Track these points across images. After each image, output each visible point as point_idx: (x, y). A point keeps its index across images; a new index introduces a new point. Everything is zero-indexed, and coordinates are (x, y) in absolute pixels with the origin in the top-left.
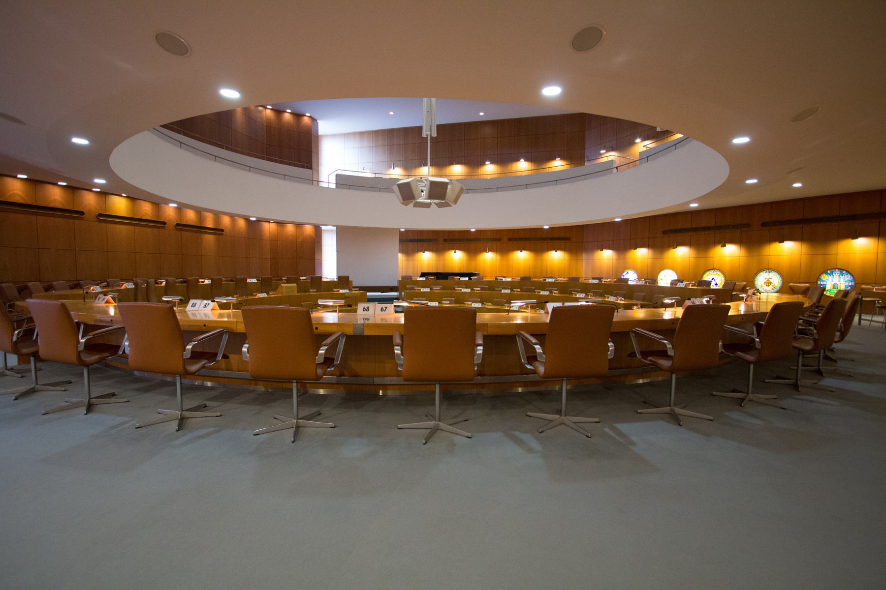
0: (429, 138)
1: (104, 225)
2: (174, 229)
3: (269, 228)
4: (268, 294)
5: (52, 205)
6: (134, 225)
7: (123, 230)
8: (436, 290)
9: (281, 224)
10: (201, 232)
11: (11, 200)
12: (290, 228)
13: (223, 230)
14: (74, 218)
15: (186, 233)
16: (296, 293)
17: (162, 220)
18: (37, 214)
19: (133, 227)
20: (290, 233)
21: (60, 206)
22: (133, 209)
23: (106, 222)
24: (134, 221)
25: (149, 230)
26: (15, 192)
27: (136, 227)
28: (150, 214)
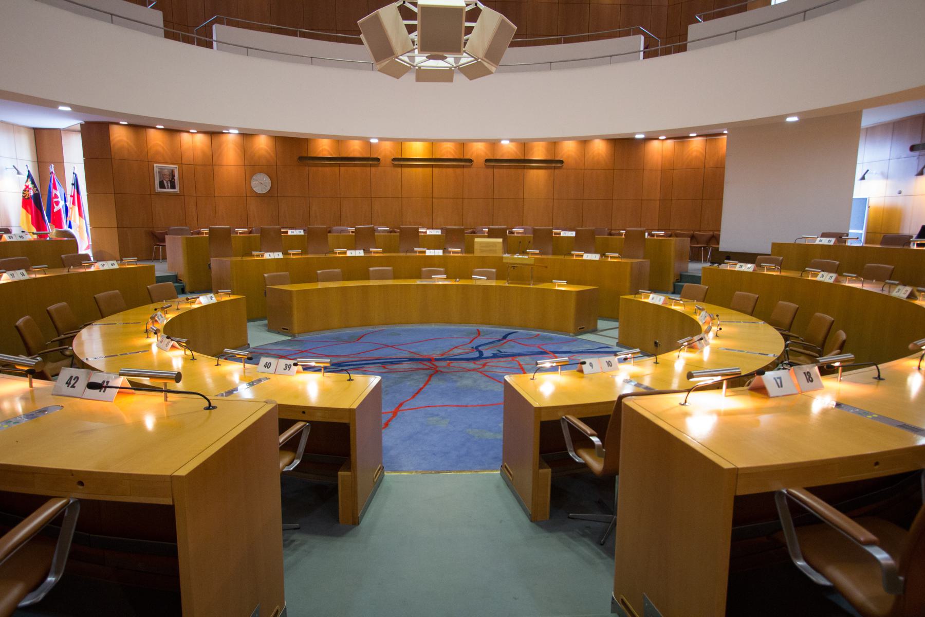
1: (399, 170)
2: (484, 166)
3: (660, 149)
4: (445, 250)
5: (351, 155)
6: (432, 166)
7: (418, 173)
8: (454, 252)
9: (681, 137)
10: (524, 168)
11: (321, 155)
12: (696, 144)
13: (562, 162)
14: (371, 165)
15: (501, 171)
16: (499, 252)
18: (339, 165)
19: (431, 169)
20: (694, 154)
21: (358, 155)
23: (402, 166)
24: (433, 162)
25: (450, 170)
26: (324, 147)
27: (434, 169)
28: (452, 151)
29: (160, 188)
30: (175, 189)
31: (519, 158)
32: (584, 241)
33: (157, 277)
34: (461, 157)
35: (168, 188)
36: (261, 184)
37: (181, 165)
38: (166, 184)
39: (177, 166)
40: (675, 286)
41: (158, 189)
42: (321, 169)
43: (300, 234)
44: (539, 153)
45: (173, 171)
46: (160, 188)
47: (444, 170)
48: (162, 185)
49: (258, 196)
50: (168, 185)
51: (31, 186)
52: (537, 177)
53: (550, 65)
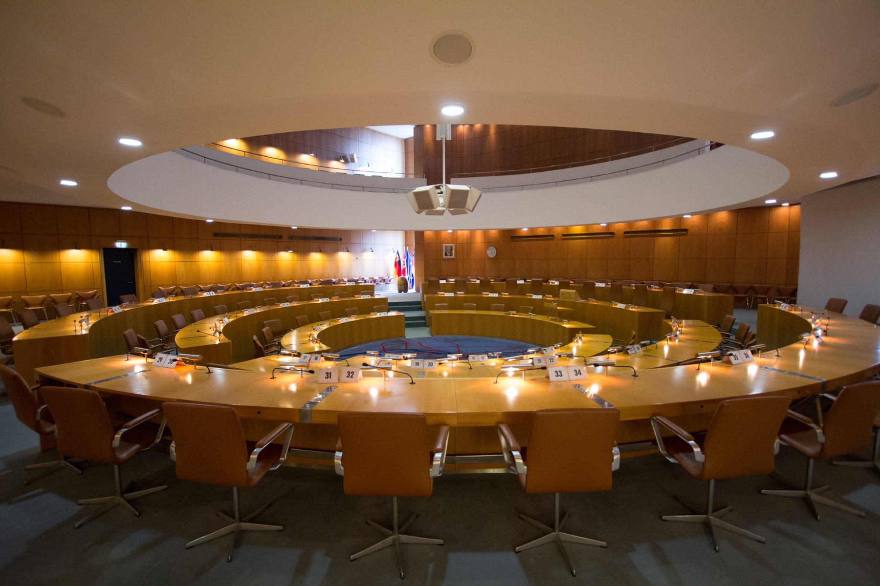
0: (444, 142)
1: (566, 241)
6: (587, 238)
10: (654, 236)
13: (686, 230)
14: (549, 240)
15: (636, 239)
17: (611, 231)
18: (532, 240)
22: (587, 229)
23: (567, 239)
24: (590, 235)
25: (600, 240)
29: (445, 256)
31: (649, 230)
32: (616, 293)
33: (389, 303)
34: (607, 231)
36: (492, 253)
37: (456, 244)
39: (454, 245)
41: (444, 257)
42: (522, 243)
44: (666, 225)
45: (452, 247)
46: (445, 256)
47: (596, 240)
48: (446, 255)
49: (490, 259)
51: (398, 257)
52: (665, 243)
53: (627, 171)
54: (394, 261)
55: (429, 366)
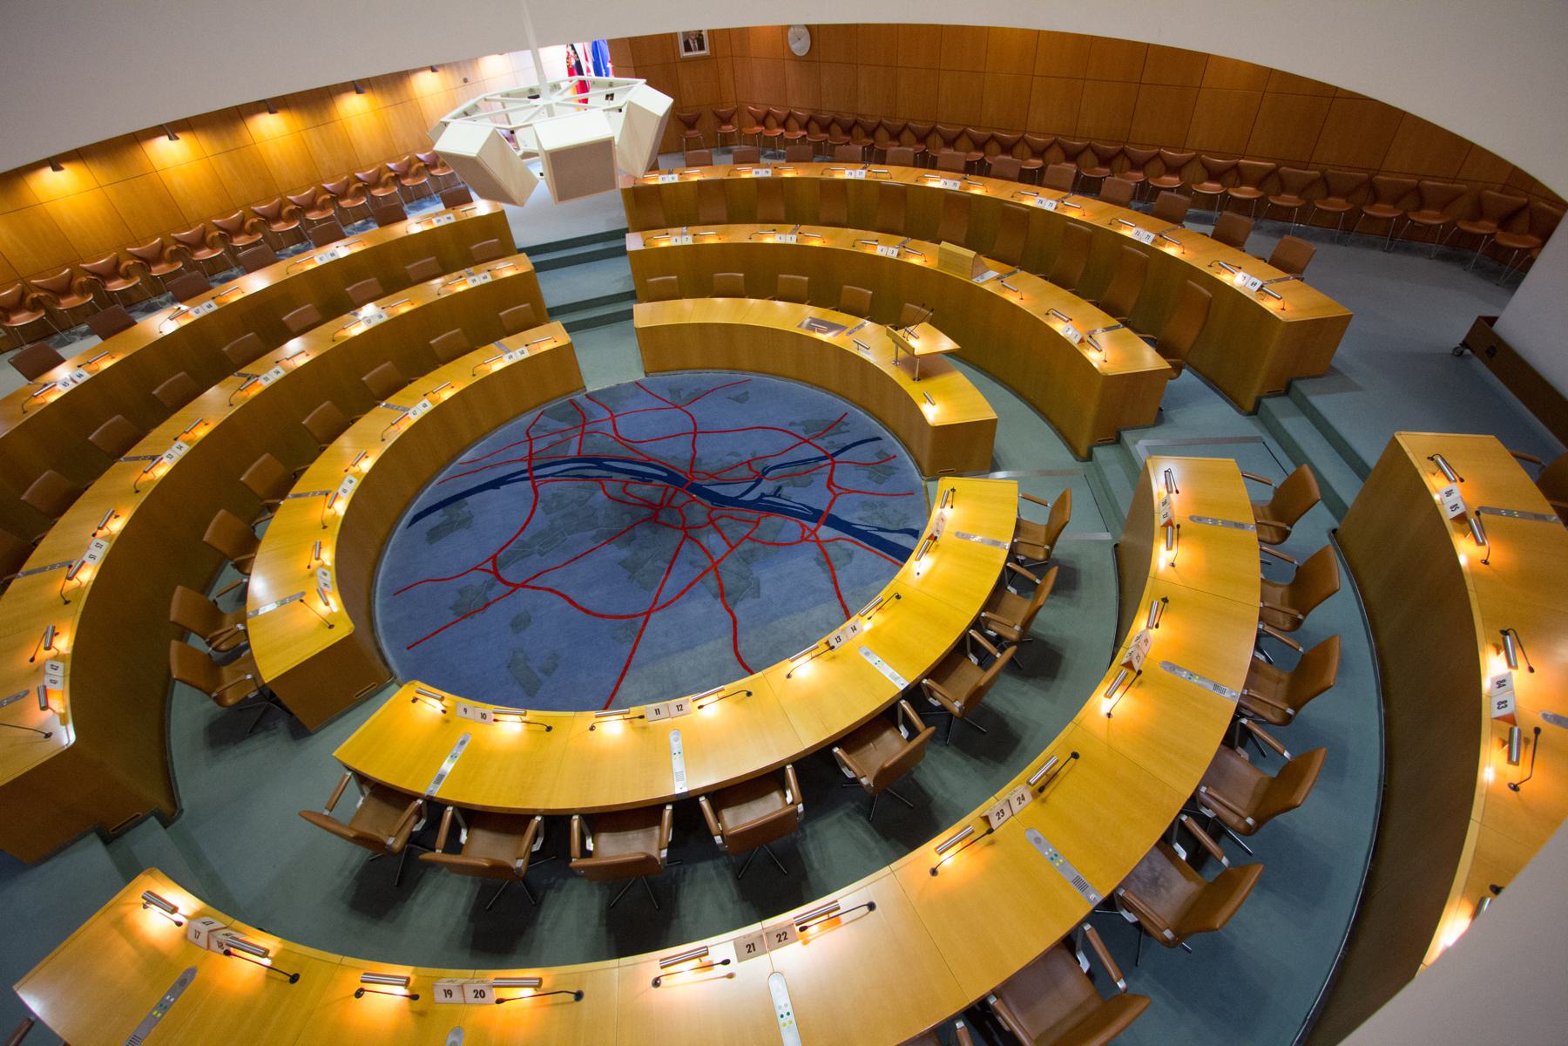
30: (701, 47)
35: (695, 50)
38: (692, 45)
40: (1258, 403)
43: (767, 175)
48: (688, 48)
50: (695, 46)
51: (572, 53)
54: (565, 65)
55: (476, 997)
